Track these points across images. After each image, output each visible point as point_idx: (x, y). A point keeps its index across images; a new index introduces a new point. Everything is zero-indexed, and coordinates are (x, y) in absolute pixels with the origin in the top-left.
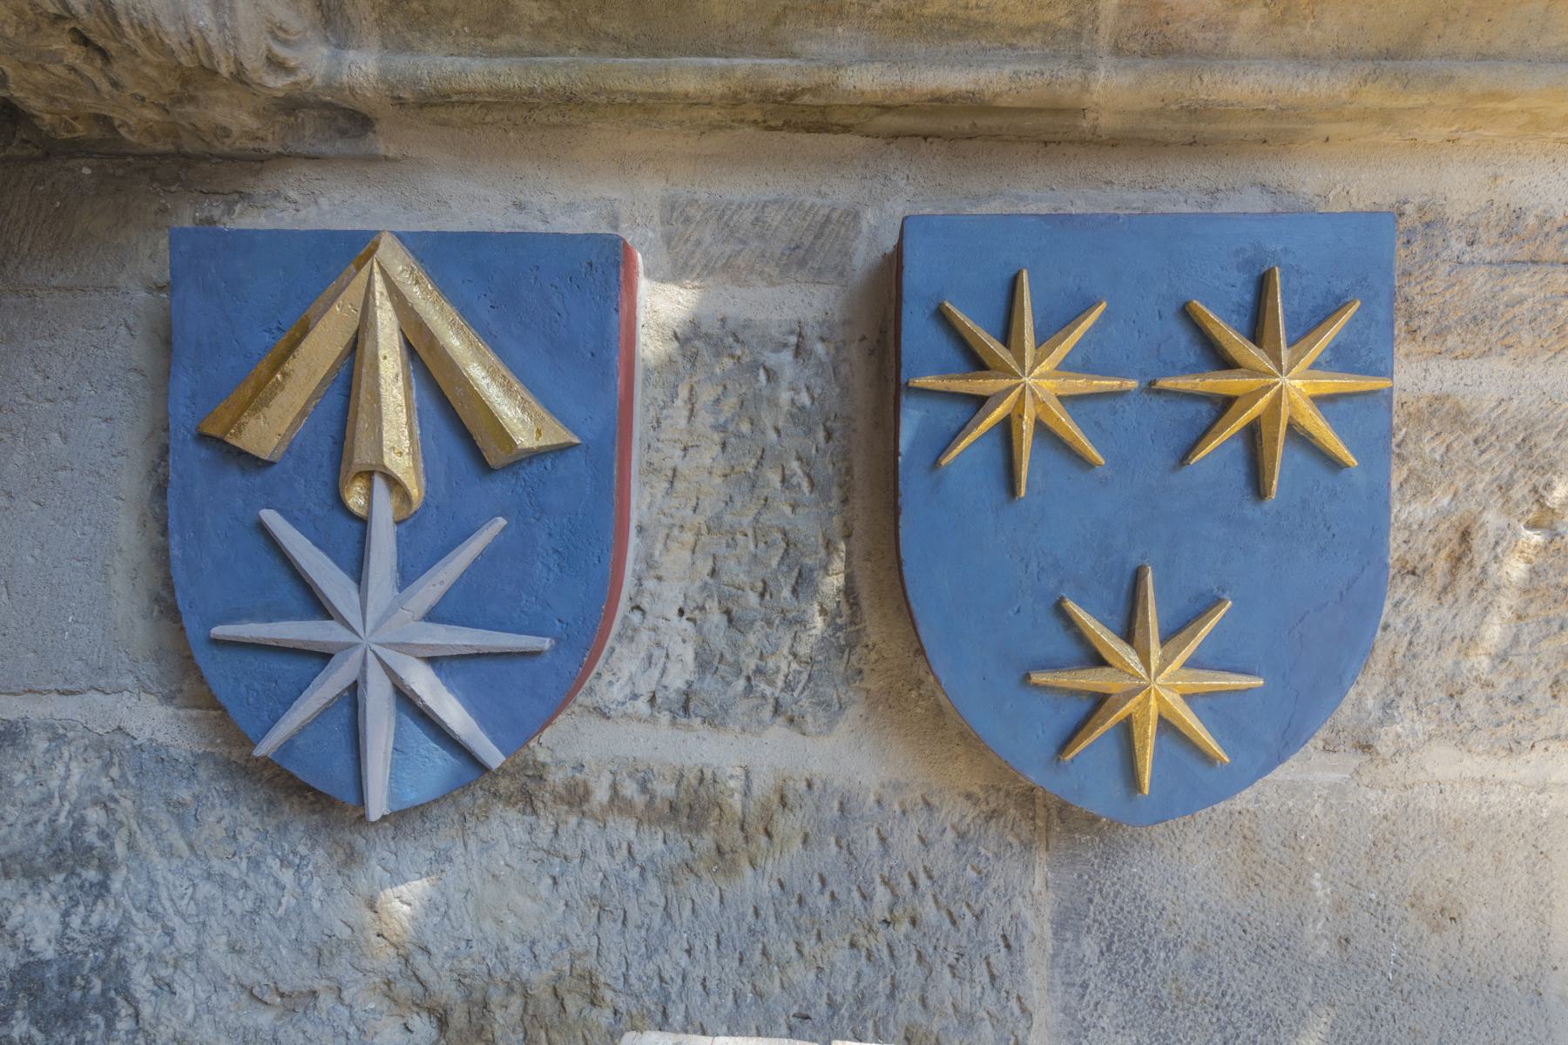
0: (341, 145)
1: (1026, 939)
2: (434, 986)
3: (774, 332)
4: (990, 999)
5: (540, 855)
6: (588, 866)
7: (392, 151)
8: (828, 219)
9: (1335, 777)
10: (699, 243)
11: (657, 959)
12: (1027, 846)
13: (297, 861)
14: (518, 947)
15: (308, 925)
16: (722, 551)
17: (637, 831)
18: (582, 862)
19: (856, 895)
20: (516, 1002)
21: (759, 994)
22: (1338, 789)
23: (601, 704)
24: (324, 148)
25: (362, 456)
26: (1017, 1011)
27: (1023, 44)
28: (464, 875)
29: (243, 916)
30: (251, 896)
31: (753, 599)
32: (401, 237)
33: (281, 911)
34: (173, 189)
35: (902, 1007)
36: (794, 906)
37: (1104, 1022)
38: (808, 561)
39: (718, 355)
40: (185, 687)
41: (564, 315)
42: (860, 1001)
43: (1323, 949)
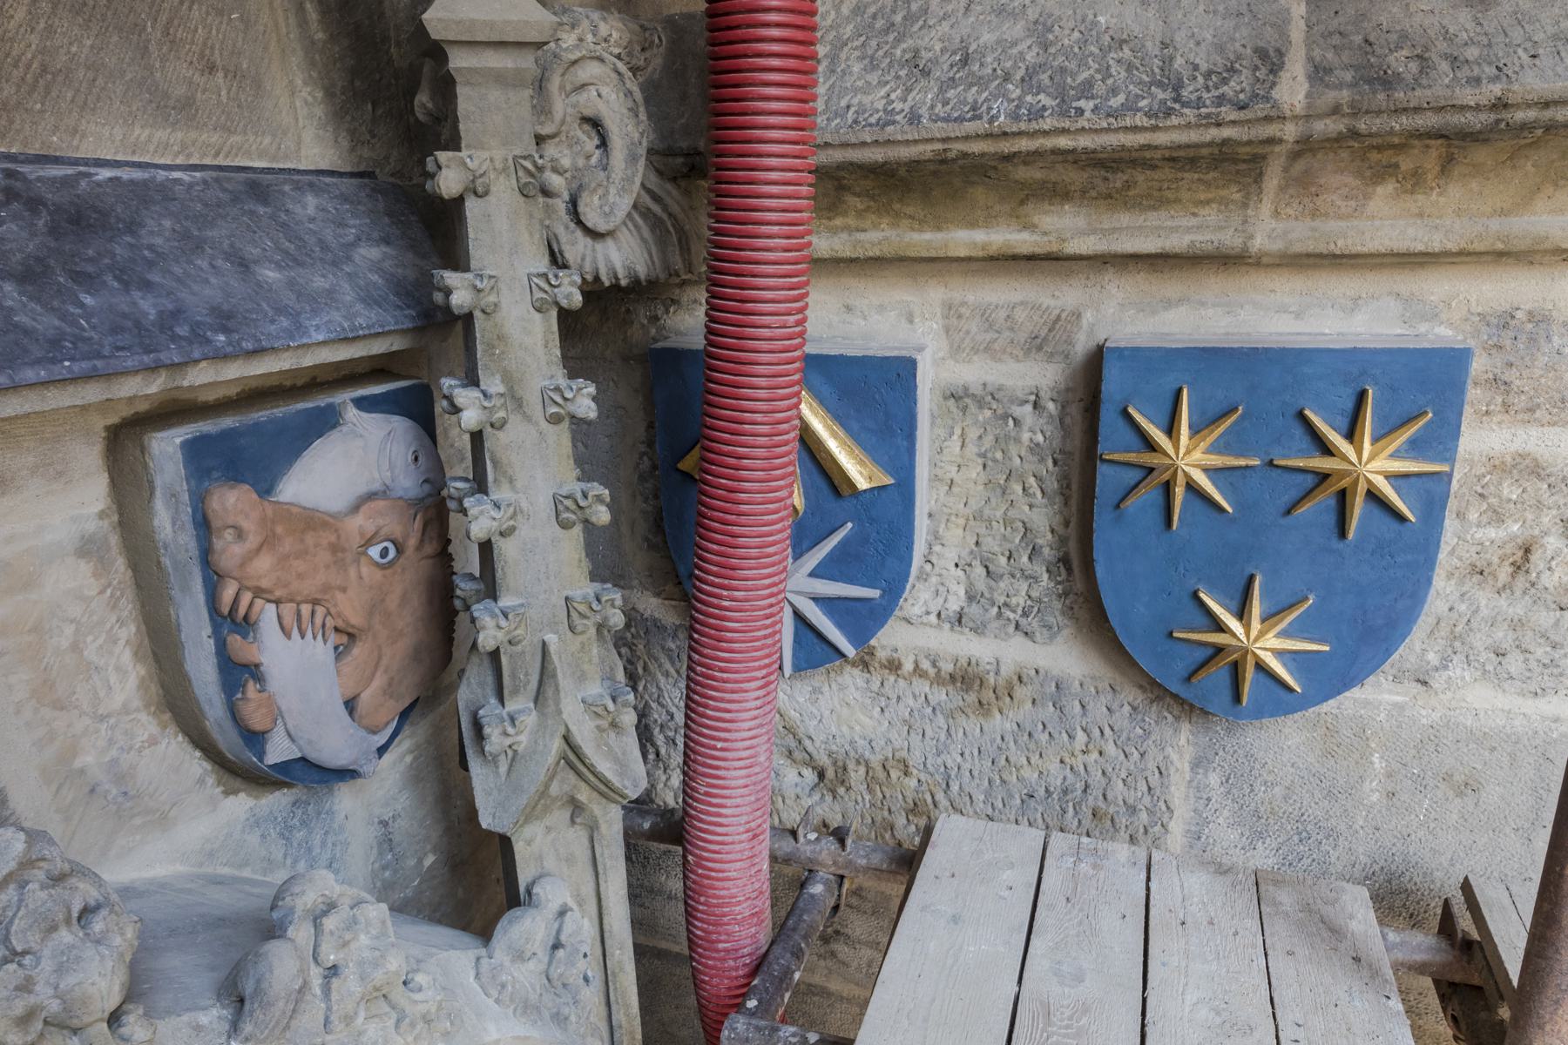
1: (1172, 771)
2: (815, 753)
3: (1020, 395)
4: (1147, 800)
8: (1059, 317)
9: (1399, 699)
10: (968, 332)
12: (1177, 718)
16: (983, 531)
19: (1065, 736)
20: (862, 770)
21: (1003, 781)
22: (1400, 707)
26: (1164, 808)
27: (1202, 212)
31: (1003, 560)
35: (1091, 798)
36: (1026, 737)
37: (1221, 820)
38: (1040, 541)
39: (981, 408)
42: (1065, 792)
43: (1375, 797)
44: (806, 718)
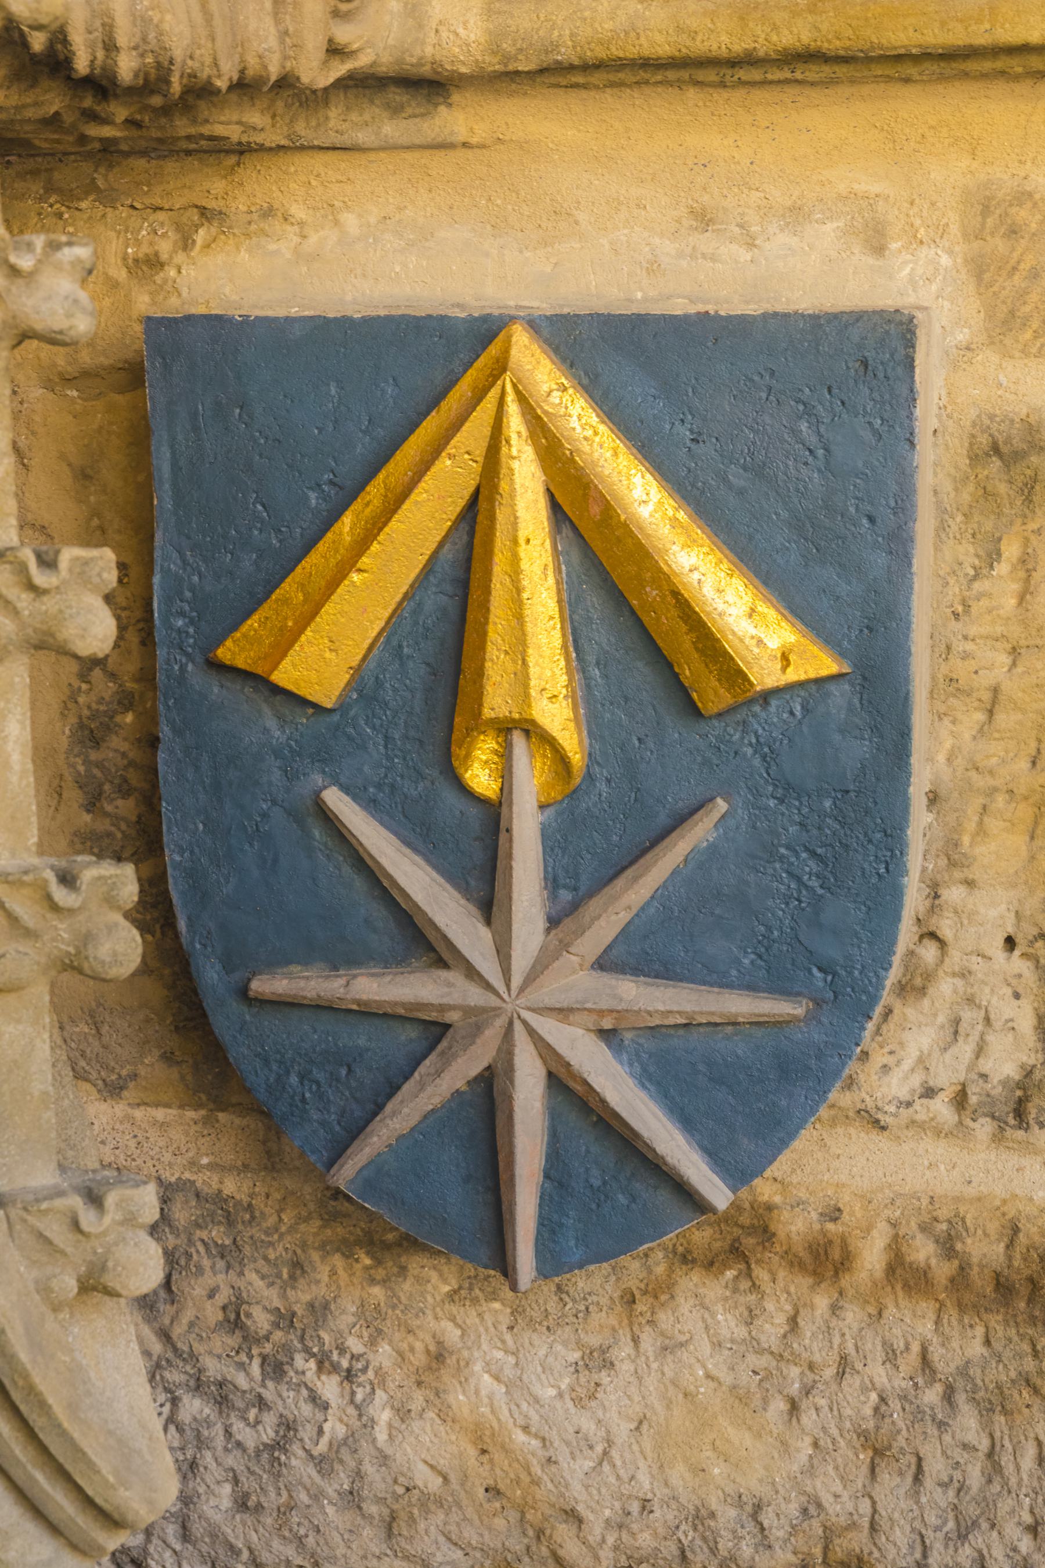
0: (391, 129)
5: (764, 1361)
6: (852, 1383)
7: (480, 133)
11: (977, 1539)
13: (345, 1364)
14: (732, 1513)
15: (368, 1468)
17: (938, 1322)
18: (841, 1375)
23: (870, 1103)
24: (362, 137)
25: (497, 702)
28: (633, 1390)
29: (258, 1453)
30: (270, 1420)
32: (533, 325)
33: (322, 1447)
34: (84, 205)
40: (142, 1071)
41: (820, 452)
44: (562, 1455)
